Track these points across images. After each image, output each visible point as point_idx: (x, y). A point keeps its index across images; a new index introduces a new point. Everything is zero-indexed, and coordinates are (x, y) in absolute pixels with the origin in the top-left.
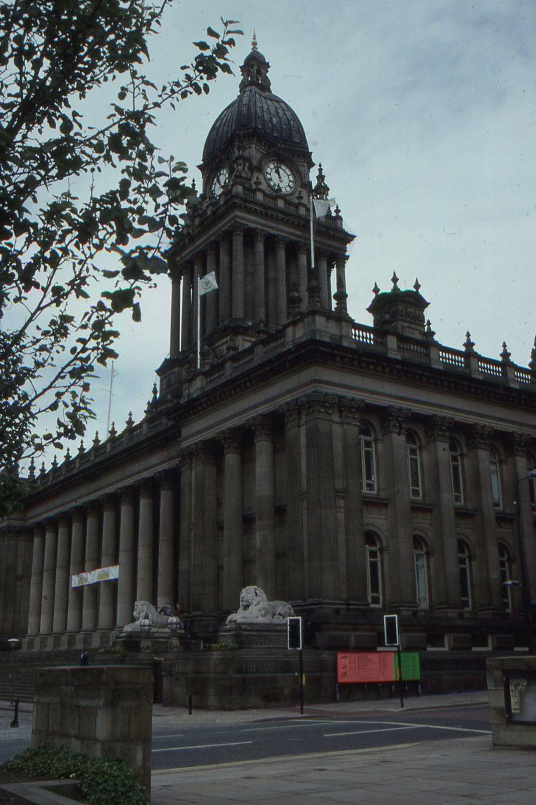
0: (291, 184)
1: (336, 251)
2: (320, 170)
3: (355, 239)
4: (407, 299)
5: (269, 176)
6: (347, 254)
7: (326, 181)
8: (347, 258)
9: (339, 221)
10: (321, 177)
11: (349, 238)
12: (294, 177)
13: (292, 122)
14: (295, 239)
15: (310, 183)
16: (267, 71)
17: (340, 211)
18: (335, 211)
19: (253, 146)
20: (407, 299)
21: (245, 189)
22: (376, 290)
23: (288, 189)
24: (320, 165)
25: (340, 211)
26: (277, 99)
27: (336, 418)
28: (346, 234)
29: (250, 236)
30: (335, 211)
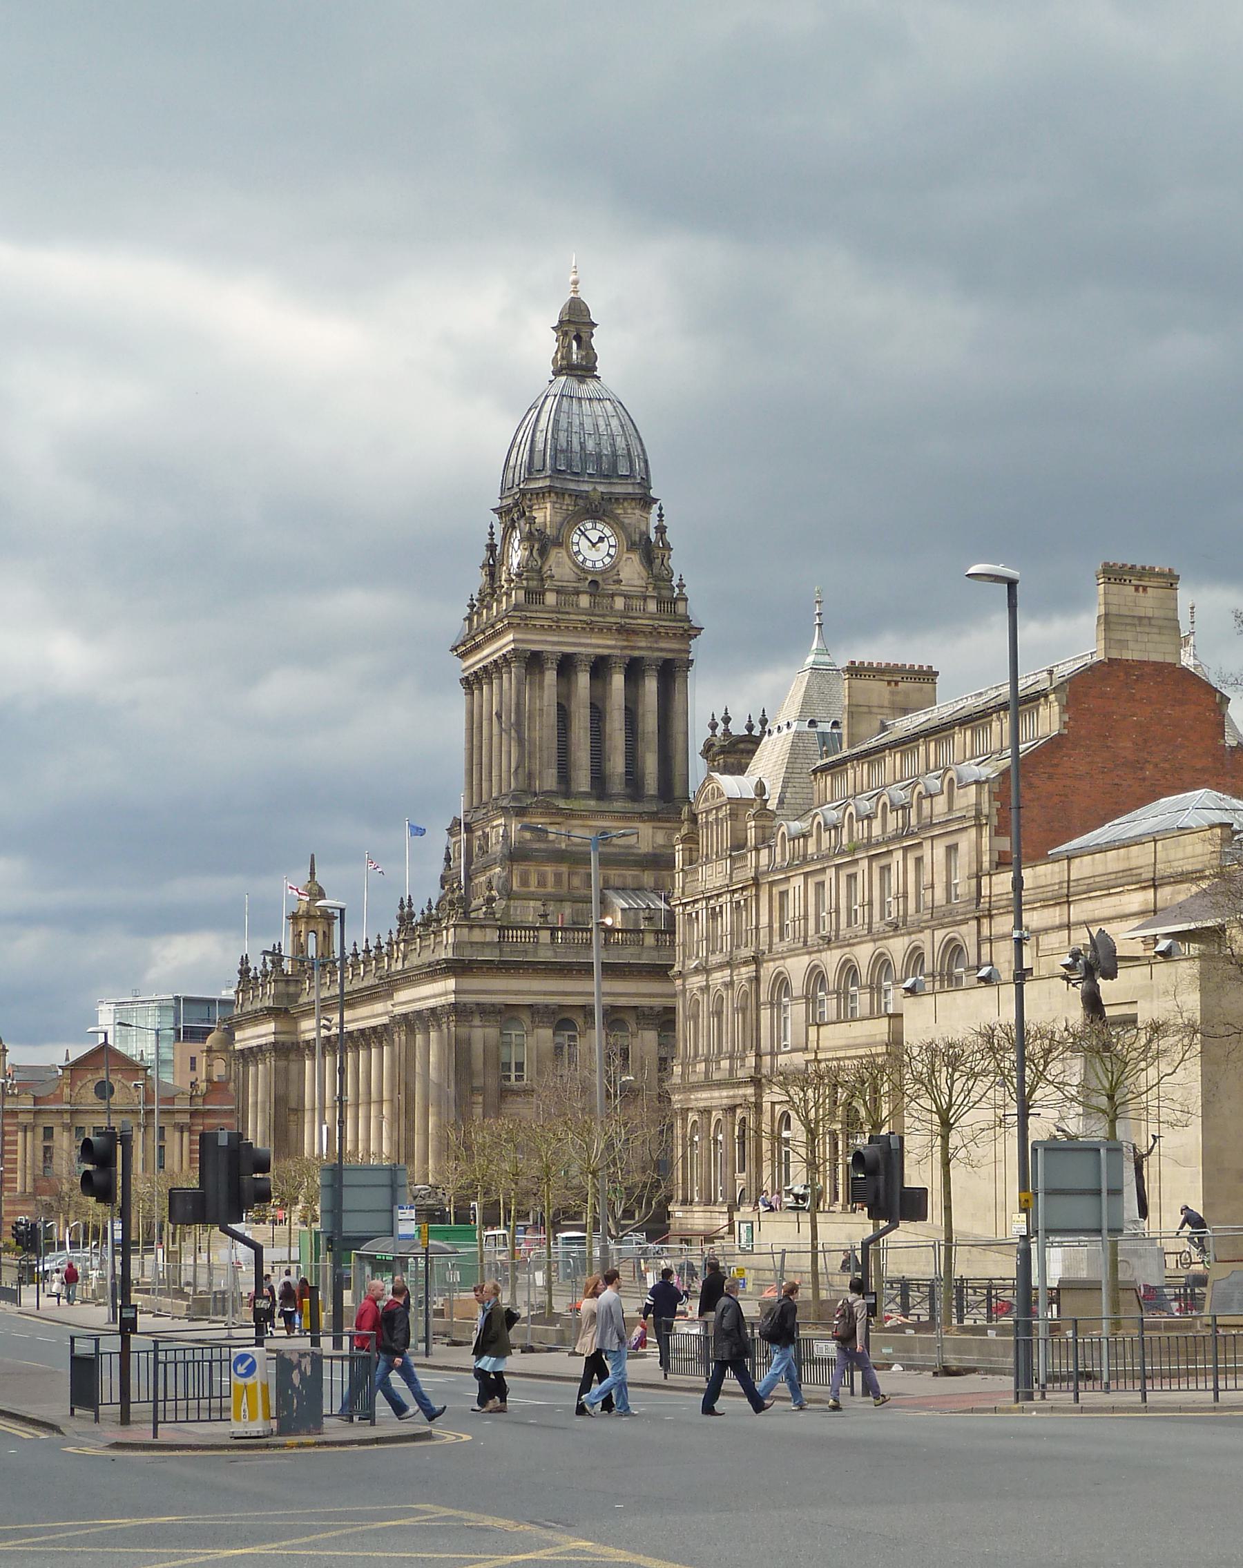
0: (612, 551)
1: (669, 656)
2: (661, 516)
4: (742, 746)
5: (575, 548)
10: (661, 530)
13: (619, 439)
14: (606, 652)
16: (592, 335)
19: (548, 505)
20: (742, 746)
21: (528, 592)
22: (714, 726)
23: (607, 560)
24: (661, 509)
27: (477, 1022)
29: (533, 662)
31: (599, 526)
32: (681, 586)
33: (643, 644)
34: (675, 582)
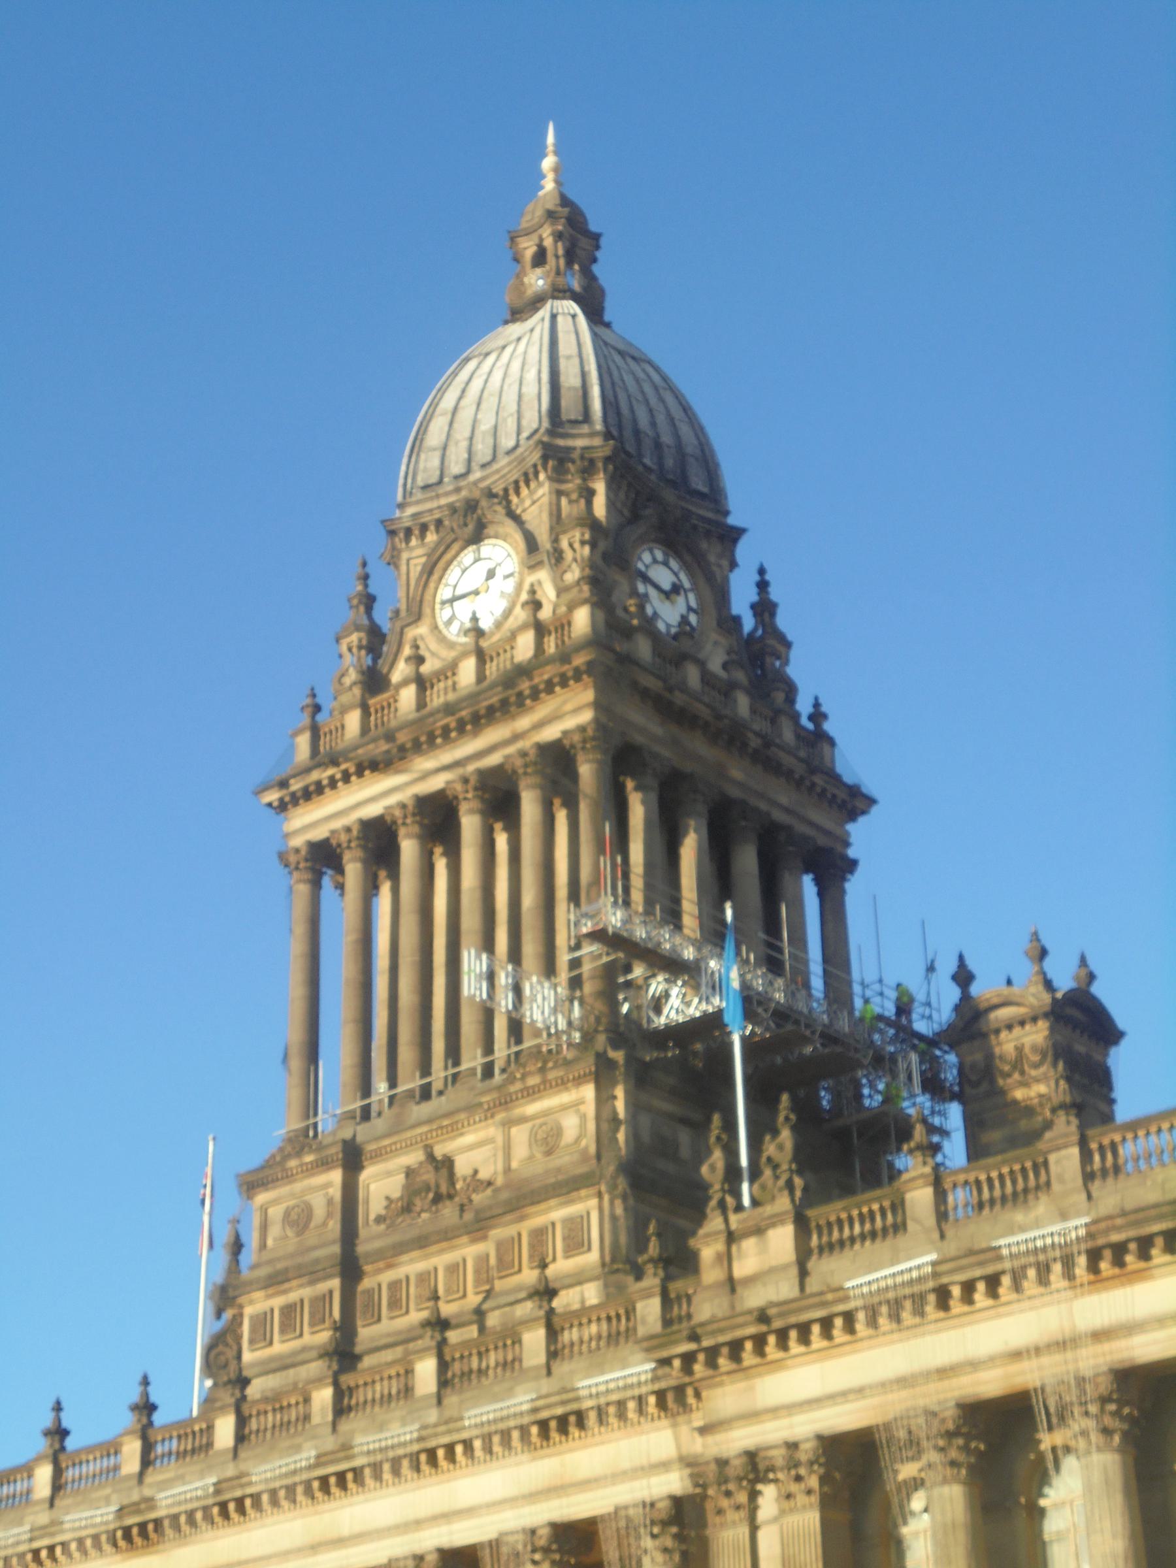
1: (822, 841)
2: (763, 586)
3: (875, 810)
6: (852, 853)
7: (782, 621)
8: (852, 865)
9: (826, 748)
10: (764, 608)
11: (854, 802)
12: (699, 598)
15: (737, 620)
17: (825, 716)
18: (811, 718)
25: (825, 716)
26: (636, 355)
28: (855, 792)
30: (811, 718)
31: (674, 564)
32: (818, 716)
33: (784, 800)
34: (804, 706)
